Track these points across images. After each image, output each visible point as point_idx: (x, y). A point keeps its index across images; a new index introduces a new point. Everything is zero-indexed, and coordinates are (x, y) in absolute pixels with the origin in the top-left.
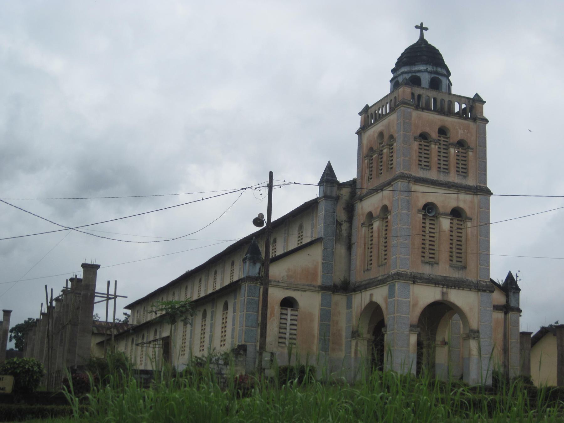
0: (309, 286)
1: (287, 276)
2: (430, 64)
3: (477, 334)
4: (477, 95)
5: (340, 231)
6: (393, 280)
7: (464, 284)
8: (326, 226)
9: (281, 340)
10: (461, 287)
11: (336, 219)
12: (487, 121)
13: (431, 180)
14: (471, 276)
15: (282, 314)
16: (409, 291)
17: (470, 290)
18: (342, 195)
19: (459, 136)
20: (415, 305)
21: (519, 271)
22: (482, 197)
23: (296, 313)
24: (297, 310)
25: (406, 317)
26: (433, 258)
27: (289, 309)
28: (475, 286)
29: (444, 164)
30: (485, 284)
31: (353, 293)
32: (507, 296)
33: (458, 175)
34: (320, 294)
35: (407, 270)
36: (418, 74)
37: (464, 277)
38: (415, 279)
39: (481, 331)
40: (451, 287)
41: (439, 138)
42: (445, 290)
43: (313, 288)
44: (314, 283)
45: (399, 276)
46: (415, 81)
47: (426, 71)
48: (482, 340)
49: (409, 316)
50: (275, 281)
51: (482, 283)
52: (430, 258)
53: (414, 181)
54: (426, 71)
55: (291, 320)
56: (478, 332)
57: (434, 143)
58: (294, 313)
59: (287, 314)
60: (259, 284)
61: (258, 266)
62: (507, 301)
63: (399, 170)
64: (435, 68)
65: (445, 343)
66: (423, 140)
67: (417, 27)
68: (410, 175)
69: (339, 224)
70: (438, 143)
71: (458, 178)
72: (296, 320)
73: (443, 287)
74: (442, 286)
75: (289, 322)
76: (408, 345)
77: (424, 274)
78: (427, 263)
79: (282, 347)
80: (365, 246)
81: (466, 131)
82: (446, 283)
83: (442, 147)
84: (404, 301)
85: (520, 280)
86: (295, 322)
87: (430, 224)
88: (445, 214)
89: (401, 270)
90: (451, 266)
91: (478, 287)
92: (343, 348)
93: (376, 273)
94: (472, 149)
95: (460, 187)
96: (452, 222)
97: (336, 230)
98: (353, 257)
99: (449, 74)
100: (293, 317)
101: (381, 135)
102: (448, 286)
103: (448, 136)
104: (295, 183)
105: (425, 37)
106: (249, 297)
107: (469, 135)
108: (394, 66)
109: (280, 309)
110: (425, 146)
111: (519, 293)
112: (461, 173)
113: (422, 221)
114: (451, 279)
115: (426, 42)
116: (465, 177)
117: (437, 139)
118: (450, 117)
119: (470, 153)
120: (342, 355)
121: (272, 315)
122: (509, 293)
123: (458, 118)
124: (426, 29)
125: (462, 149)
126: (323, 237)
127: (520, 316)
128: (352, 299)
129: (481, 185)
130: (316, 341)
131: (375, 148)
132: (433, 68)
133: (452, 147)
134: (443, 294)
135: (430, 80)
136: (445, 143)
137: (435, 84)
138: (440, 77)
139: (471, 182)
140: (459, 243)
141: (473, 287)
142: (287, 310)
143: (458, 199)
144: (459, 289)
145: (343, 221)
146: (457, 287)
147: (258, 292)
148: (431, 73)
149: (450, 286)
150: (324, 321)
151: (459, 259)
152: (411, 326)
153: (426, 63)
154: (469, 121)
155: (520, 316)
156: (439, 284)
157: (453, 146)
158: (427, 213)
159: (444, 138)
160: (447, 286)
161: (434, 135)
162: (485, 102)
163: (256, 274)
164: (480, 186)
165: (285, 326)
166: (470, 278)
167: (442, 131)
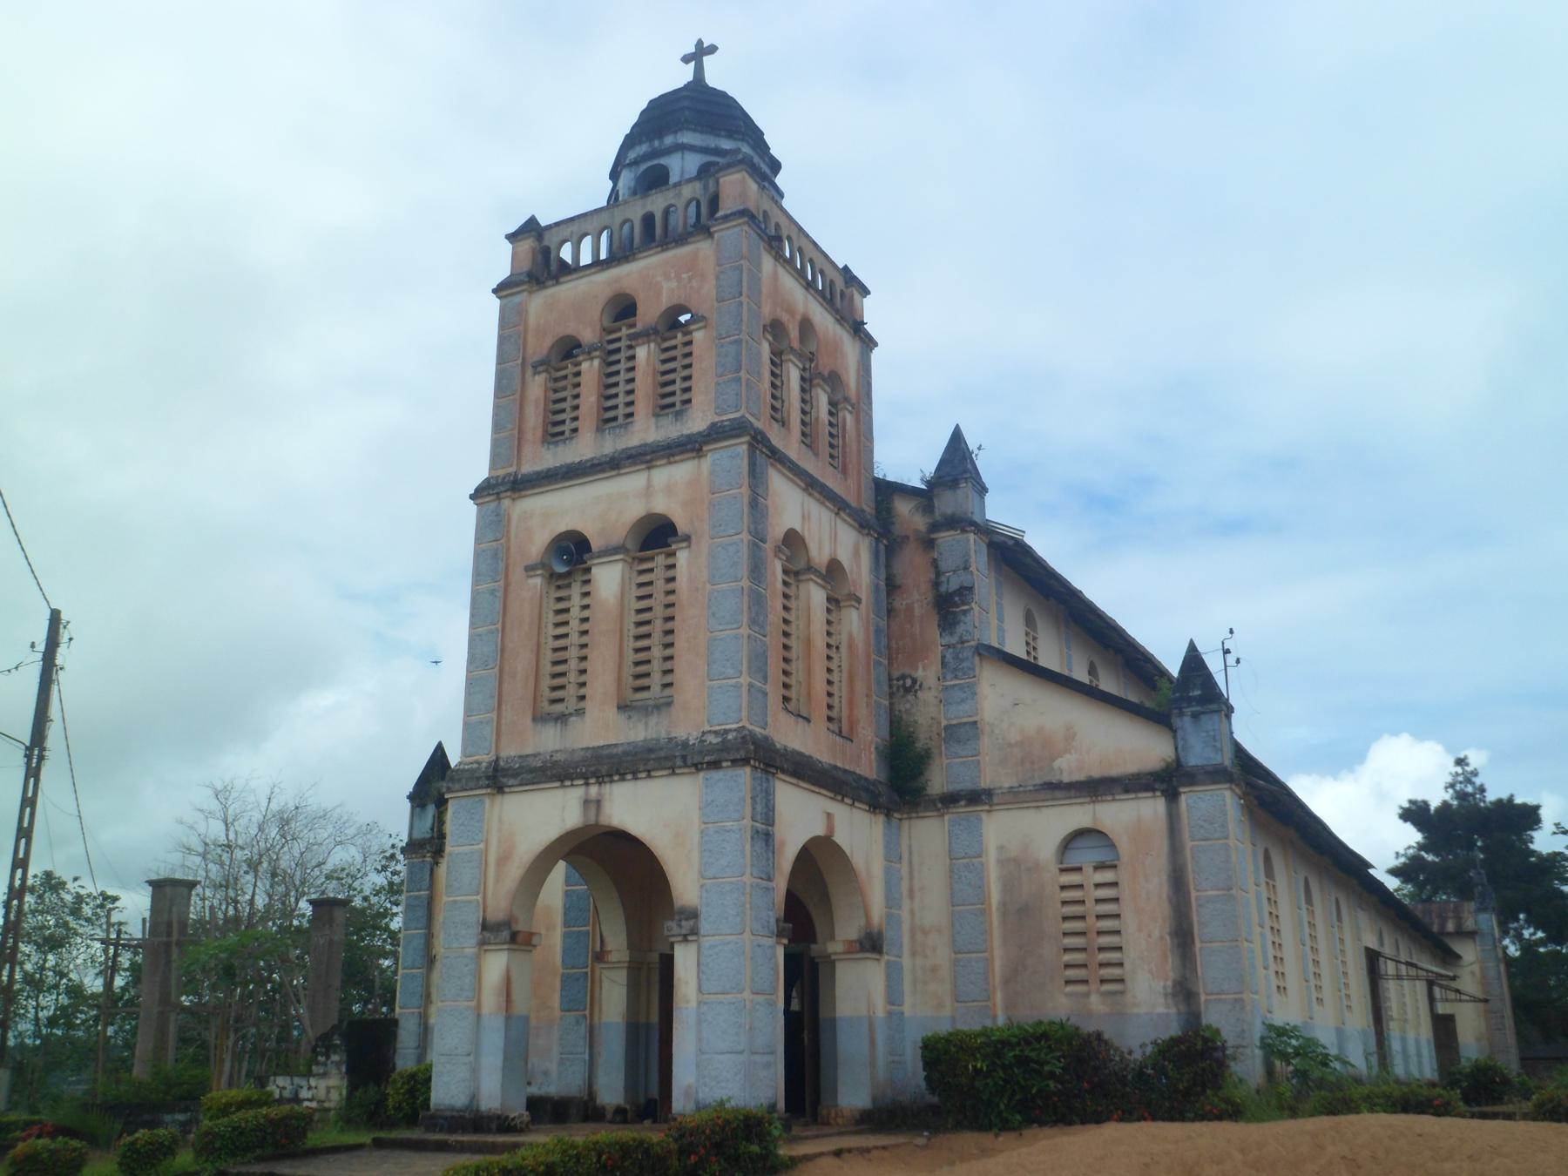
3: (691, 923)
17: (674, 773)
19: (664, 300)
20: (504, 859)
21: (1231, 632)
22: (717, 455)
25: (470, 902)
28: (684, 758)
32: (1173, 731)
40: (611, 776)
42: (594, 790)
48: (706, 942)
57: (586, 357)
60: (429, 855)
61: (431, 810)
65: (872, 944)
67: (686, 59)
71: (657, 427)
73: (587, 784)
74: (581, 782)
77: (535, 755)
81: (684, 276)
82: (592, 769)
84: (466, 854)
85: (1238, 661)
95: (653, 452)
106: (412, 894)
107: (694, 283)
118: (634, 260)
122: (1176, 722)
123: (659, 249)
124: (712, 49)
129: (724, 418)
133: (639, 345)
134: (586, 802)
138: (663, 161)
139: (697, 421)
141: (679, 762)
144: (635, 778)
146: (630, 773)
147: (427, 877)
149: (607, 776)
150: (574, 927)
152: (485, 926)
154: (694, 242)
157: (640, 341)
160: (598, 777)
161: (588, 335)
163: (427, 832)
166: (680, 733)
167: (624, 308)
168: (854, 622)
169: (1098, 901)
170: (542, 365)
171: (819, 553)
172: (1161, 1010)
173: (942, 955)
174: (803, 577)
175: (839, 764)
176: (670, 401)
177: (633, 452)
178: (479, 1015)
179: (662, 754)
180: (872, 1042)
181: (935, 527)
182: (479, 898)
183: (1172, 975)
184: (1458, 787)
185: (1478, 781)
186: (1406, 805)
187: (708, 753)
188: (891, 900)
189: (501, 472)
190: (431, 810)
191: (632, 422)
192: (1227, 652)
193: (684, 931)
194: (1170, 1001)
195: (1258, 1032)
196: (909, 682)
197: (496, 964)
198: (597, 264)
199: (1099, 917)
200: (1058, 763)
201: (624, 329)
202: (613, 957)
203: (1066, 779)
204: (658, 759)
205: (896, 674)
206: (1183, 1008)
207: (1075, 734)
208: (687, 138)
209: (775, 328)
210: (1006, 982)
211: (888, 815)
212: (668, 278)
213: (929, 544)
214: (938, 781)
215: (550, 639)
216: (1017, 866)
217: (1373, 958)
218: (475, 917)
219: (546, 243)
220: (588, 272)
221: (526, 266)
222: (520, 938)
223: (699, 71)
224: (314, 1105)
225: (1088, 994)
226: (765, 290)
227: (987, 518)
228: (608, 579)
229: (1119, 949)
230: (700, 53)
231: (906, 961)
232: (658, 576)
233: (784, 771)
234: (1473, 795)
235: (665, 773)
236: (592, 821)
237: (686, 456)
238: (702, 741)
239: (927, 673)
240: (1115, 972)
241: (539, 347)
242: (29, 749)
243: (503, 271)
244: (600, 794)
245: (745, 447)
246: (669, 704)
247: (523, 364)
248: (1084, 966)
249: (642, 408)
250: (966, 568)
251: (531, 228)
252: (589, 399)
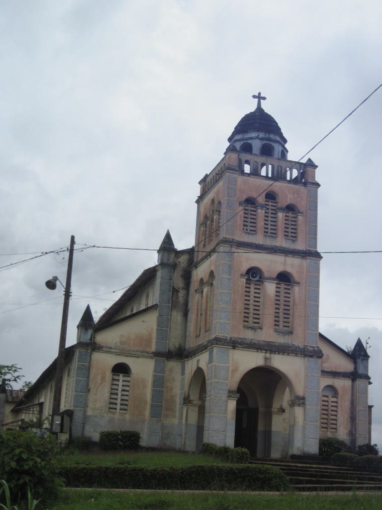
0: (142, 352)
1: (121, 342)
2: (262, 132)
3: (303, 401)
4: (309, 160)
5: (177, 298)
6: (212, 345)
7: (289, 349)
8: (162, 293)
9: (111, 406)
10: (285, 352)
11: (173, 287)
12: (318, 185)
13: (255, 244)
14: (297, 341)
15: (113, 380)
16: (228, 356)
17: (296, 356)
18: (180, 262)
20: (235, 370)
21: (369, 338)
23: (128, 379)
24: (129, 376)
26: (258, 323)
27: (121, 375)
28: (301, 352)
29: (271, 229)
30: (312, 349)
31: (186, 359)
32: (355, 363)
33: (286, 239)
34: (154, 360)
35: (228, 334)
36: (249, 141)
37: (290, 342)
38: (235, 344)
40: (275, 352)
41: (267, 203)
42: (268, 355)
43: (147, 355)
44: (148, 350)
45: (218, 341)
46: (247, 148)
47: (257, 138)
48: (307, 407)
49: (227, 382)
50: (107, 347)
51: (309, 348)
52: (254, 323)
53: (237, 246)
54: (257, 138)
55: (123, 386)
56: (303, 398)
58: (126, 379)
59: (118, 380)
61: (90, 332)
62: (355, 368)
63: (223, 234)
64: (267, 134)
66: (249, 206)
67: (254, 97)
68: (233, 239)
69: (175, 291)
70: (265, 207)
72: (129, 386)
74: (264, 351)
75: (120, 388)
76: (226, 410)
77: (245, 339)
78: (250, 327)
79: (114, 413)
80: (197, 311)
82: (269, 348)
83: (270, 211)
85: (370, 347)
86: (127, 388)
87: (255, 288)
88: (271, 279)
89: (220, 334)
90: (276, 331)
91: (304, 352)
92: (177, 414)
93: (203, 340)
94: (302, 213)
96: (279, 286)
97: (172, 297)
98: (189, 324)
99: (285, 141)
100: (125, 383)
101: (213, 201)
102: (271, 352)
103: (277, 201)
104: (94, 246)
105: (263, 106)
107: (299, 199)
108: (230, 134)
109: (111, 375)
110: (252, 211)
111: (367, 360)
112: (290, 238)
113: (245, 285)
114: (275, 344)
115: (262, 110)
116: (293, 241)
117: (264, 204)
119: (300, 218)
120: (176, 421)
121: (104, 381)
124: (264, 98)
125: (292, 213)
126: (158, 304)
127: (370, 383)
128: (185, 365)
129: (311, 249)
130: (148, 407)
131: (208, 215)
132: (265, 135)
133: (280, 212)
134: (266, 359)
135: (261, 146)
136: (273, 208)
137: (267, 151)
138: (272, 144)
139: (300, 246)
140: (286, 308)
141: (299, 353)
142: (119, 375)
143: (285, 263)
144: (283, 354)
145: (181, 288)
147: (89, 358)
148: (262, 139)
151: (286, 324)
152: (230, 392)
153: (258, 130)
155: (370, 383)
156: (261, 349)
158: (251, 278)
159: (272, 202)
161: (261, 200)
162: (317, 167)
164: (309, 250)
165: (116, 391)
166: (296, 344)
167: (271, 196)
169: (332, 406)
177: (280, 248)
179: (293, 349)
183: (349, 429)
190: (90, 332)
191: (275, 237)
192: (368, 343)
193: (300, 403)
194: (348, 436)
198: (267, 177)
199: (332, 411)
201: (270, 202)
202: (195, 402)
203: (326, 370)
204: (292, 350)
212: (290, 194)
220: (261, 178)
223: (259, 104)
225: (327, 431)
228: (270, 288)
229: (336, 420)
232: (282, 291)
235: (294, 355)
237: (300, 257)
240: (334, 426)
244: (270, 357)
246: (291, 333)
248: (327, 424)
249: (280, 233)
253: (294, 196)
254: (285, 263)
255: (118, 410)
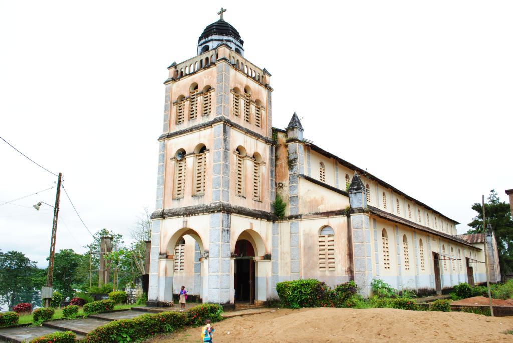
17: (204, 214)
20: (165, 236)
22: (216, 127)
27: (180, 245)
38: (163, 216)
39: (210, 252)
42: (186, 218)
48: (211, 259)
58: (183, 248)
65: (267, 257)
81: (210, 77)
122: (350, 195)
124: (225, 10)
139: (212, 118)
144: (195, 215)
152: (160, 254)
161: (187, 95)
168: (264, 170)
170: (176, 103)
171: (250, 151)
172: (344, 276)
173: (288, 260)
174: (245, 158)
175: (257, 209)
176: (206, 113)
178: (159, 277)
180: (267, 284)
181: (288, 142)
182: (159, 247)
184: (492, 199)
185: (497, 197)
186: (474, 205)
187: (211, 209)
188: (273, 245)
189: (165, 133)
195: (369, 281)
196: (281, 185)
197: (164, 263)
200: (318, 208)
203: (321, 212)
205: (277, 183)
206: (350, 275)
207: (324, 199)
208: (214, 37)
209: (236, 90)
210: (304, 267)
211: (274, 222)
212: (206, 78)
213: (286, 146)
214: (287, 212)
215: (178, 178)
216: (308, 236)
217: (436, 257)
218: (158, 252)
219: (177, 69)
221: (172, 76)
222: (169, 257)
223: (222, 17)
224: (135, 296)
225: (325, 271)
226: (231, 79)
227: (304, 137)
228: (190, 161)
230: (223, 11)
231: (279, 262)
233: (235, 213)
234: (496, 201)
236: (185, 227)
238: (210, 206)
239: (286, 183)
241: (175, 98)
242: (55, 208)
243: (167, 78)
245: (223, 124)
247: (171, 102)
249: (199, 114)
250: (296, 153)
251: (174, 65)
252: (186, 112)
253: (208, 78)
254: (200, 137)
255: (179, 271)
